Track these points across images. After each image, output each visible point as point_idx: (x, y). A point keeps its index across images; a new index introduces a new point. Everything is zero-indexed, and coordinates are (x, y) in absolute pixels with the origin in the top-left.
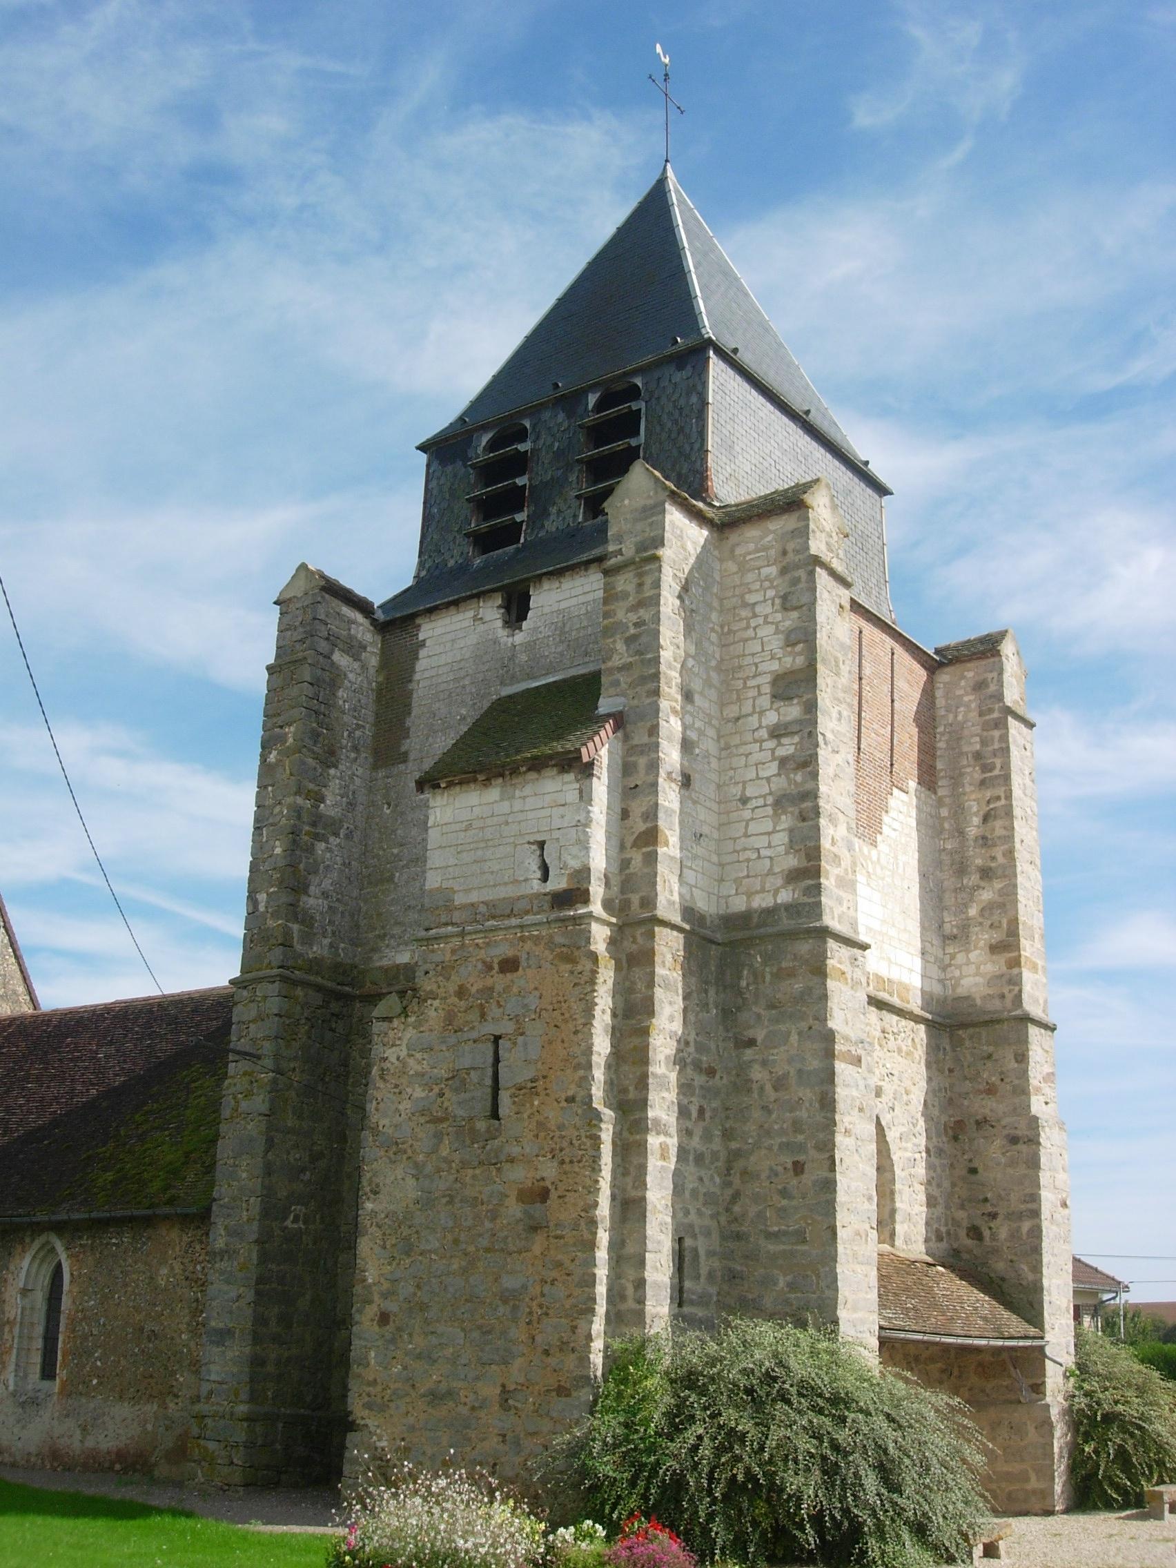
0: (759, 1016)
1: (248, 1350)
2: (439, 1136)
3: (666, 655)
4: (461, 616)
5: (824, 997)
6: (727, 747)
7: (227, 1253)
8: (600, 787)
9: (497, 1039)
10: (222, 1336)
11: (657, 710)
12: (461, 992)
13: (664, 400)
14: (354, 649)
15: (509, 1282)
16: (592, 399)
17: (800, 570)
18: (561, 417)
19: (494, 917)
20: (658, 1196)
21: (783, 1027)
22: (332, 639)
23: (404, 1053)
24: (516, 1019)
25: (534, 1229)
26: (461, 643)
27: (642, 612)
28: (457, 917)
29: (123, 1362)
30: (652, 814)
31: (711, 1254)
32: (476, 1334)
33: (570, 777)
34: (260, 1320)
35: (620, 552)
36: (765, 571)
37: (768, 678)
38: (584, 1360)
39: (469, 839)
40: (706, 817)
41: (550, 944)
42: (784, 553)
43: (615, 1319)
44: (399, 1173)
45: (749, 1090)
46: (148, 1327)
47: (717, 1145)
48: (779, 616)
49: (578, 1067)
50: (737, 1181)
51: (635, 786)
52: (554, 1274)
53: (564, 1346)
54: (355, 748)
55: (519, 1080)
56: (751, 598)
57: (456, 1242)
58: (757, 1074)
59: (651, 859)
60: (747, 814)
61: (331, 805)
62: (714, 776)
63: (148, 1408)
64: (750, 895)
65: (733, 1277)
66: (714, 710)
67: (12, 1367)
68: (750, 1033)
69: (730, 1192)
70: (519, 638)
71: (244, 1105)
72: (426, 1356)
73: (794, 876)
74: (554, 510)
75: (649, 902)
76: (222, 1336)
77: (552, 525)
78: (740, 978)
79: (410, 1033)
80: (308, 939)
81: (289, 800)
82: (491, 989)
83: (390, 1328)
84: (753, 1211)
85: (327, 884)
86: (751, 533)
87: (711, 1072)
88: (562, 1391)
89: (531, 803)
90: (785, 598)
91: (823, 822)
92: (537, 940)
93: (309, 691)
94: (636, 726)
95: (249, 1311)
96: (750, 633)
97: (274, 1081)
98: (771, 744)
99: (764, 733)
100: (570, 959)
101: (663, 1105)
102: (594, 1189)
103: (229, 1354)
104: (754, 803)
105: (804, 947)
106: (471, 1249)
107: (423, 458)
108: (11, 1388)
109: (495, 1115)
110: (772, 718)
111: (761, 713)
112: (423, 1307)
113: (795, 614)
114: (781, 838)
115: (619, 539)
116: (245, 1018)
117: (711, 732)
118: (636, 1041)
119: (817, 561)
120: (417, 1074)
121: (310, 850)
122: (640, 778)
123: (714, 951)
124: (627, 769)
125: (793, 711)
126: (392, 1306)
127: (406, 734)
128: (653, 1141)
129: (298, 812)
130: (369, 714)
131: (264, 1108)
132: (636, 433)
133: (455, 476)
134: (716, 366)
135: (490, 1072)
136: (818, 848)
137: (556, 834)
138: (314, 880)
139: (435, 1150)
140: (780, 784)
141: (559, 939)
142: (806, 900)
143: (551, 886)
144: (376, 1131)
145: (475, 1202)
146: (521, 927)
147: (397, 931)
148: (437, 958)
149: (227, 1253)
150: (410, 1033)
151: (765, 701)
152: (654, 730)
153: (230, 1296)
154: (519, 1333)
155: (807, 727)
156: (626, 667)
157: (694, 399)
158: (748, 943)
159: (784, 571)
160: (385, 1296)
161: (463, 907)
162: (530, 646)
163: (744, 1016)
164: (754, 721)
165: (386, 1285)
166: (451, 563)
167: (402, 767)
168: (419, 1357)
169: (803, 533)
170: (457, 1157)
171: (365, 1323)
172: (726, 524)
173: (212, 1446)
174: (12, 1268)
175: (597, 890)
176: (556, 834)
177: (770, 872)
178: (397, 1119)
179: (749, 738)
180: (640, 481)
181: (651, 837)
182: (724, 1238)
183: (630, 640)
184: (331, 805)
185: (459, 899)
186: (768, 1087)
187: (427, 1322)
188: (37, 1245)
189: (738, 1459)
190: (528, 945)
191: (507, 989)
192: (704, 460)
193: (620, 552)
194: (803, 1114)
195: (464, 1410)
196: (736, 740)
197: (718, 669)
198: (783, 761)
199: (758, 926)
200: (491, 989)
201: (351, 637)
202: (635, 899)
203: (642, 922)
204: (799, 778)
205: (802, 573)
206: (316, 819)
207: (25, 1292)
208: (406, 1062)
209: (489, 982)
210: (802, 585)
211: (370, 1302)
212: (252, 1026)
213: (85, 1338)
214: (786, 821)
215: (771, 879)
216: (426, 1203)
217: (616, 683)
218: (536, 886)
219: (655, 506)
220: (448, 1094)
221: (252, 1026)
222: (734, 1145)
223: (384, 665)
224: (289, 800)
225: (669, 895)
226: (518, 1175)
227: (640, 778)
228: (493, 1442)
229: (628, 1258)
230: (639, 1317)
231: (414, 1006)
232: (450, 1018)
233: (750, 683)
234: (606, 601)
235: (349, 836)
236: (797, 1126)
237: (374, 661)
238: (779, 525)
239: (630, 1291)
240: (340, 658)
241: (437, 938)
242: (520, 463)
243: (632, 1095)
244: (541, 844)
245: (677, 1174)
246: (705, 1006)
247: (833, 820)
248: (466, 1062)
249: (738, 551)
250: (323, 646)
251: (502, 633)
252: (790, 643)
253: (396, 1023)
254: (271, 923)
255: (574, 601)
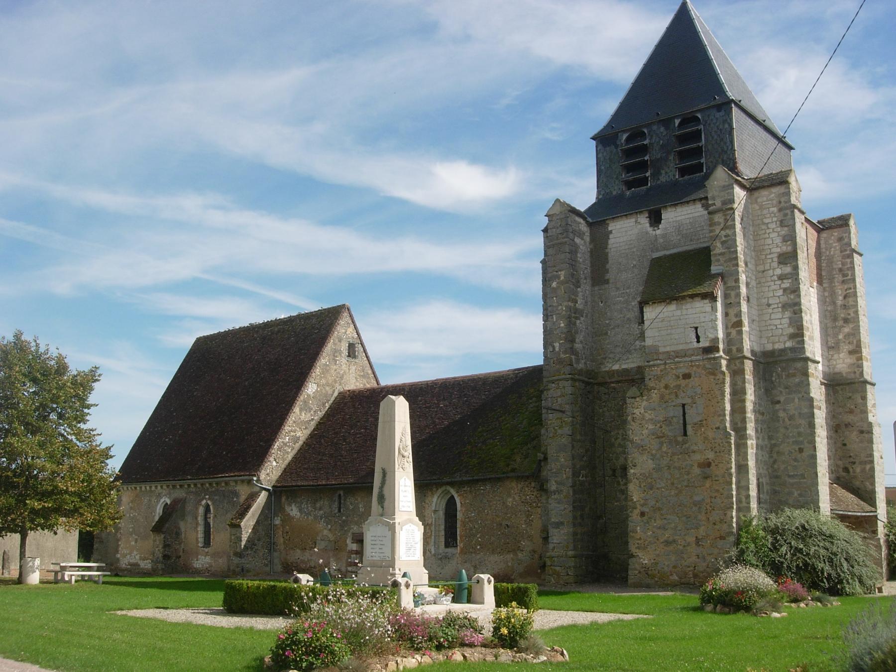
0: (781, 392)
1: (571, 530)
2: (662, 443)
3: (739, 249)
4: (628, 221)
5: (809, 384)
6: (760, 283)
7: (558, 491)
8: (719, 305)
9: (684, 405)
10: (558, 525)
11: (738, 272)
12: (666, 387)
13: (712, 125)
14: (581, 235)
15: (696, 498)
16: (677, 122)
17: (788, 210)
18: (662, 129)
19: (677, 357)
20: (751, 463)
21: (791, 396)
22: (574, 232)
23: (642, 411)
24: (692, 397)
25: (706, 478)
26: (630, 233)
27: (727, 231)
28: (661, 357)
29: (493, 538)
30: (739, 314)
31: (767, 484)
32: (684, 518)
33: (707, 301)
34: (575, 518)
35: (714, 204)
36: (772, 209)
37: (776, 255)
38: (731, 526)
39: (669, 325)
40: (755, 312)
41: (704, 368)
42: (780, 202)
43: (739, 510)
44: (645, 458)
45: (778, 421)
46: (504, 523)
47: (766, 442)
48: (779, 229)
49: (719, 416)
50: (775, 455)
51: (731, 304)
52: (716, 494)
53: (721, 521)
54: (586, 279)
55: (695, 421)
56: (766, 221)
57: (673, 484)
58: (781, 414)
59: (740, 333)
60: (770, 311)
61: (580, 305)
62: (755, 295)
63: (508, 556)
64: (773, 343)
65: (775, 492)
66: (754, 268)
67: (432, 543)
68: (778, 398)
69: (772, 460)
70: (658, 232)
71: (559, 431)
72: (663, 528)
73: (792, 336)
74: (663, 172)
75: (740, 350)
76: (558, 525)
77: (663, 178)
78: (772, 376)
79: (644, 403)
80: (578, 361)
81: (566, 303)
82: (680, 386)
83: (646, 517)
84: (782, 467)
85: (581, 338)
86: (764, 192)
87: (763, 414)
88: (722, 538)
89: (690, 311)
90: (781, 221)
91: (803, 314)
92: (698, 366)
93: (568, 256)
94: (729, 277)
95: (571, 514)
96: (767, 235)
97: (573, 422)
98: (779, 282)
99: (775, 278)
100: (714, 374)
101: (751, 430)
102: (730, 462)
103: (562, 532)
104: (773, 306)
105: (799, 365)
106: (679, 486)
107: (594, 143)
108: (433, 552)
109: (685, 434)
110: (778, 272)
111: (774, 269)
112: (659, 509)
113: (786, 229)
114: (786, 321)
115: (714, 198)
116: (555, 395)
117: (754, 278)
118: (740, 404)
119: (794, 207)
120: (649, 419)
121: (575, 324)
122: (732, 300)
123: (761, 366)
124: (726, 296)
125: (788, 269)
126: (646, 509)
127: (607, 271)
128: (749, 442)
129: (569, 308)
130: (588, 262)
131: (570, 433)
132: (700, 139)
133: (611, 152)
134: (735, 111)
135: (682, 418)
136: (802, 325)
137: (703, 324)
138: (577, 336)
139: (660, 448)
140: (784, 299)
141: (708, 366)
142: (797, 346)
143: (701, 345)
144: (632, 442)
145: (679, 468)
146: (691, 361)
147: (611, 356)
148: (654, 373)
149: (558, 491)
150: (644, 403)
151: (775, 264)
152: (737, 280)
153: (559, 507)
154: (702, 517)
155: (794, 275)
156: (722, 254)
157: (727, 126)
158: (776, 362)
159: (780, 210)
160: (642, 506)
161: (664, 353)
162: (664, 236)
163: (774, 392)
164: (771, 272)
165: (642, 502)
166: (614, 193)
167: (607, 286)
168: (659, 528)
169: (788, 194)
170: (670, 451)
171: (635, 516)
172: (753, 187)
173: (558, 568)
174: (427, 501)
175: (721, 346)
176: (703, 324)
177: (782, 335)
178: (642, 437)
179: (769, 279)
180: (720, 174)
181: (739, 324)
182: (771, 478)
183: (723, 243)
184: (580, 305)
185: (661, 350)
186: (786, 419)
187: (662, 515)
188: (440, 491)
189: (799, 558)
190: (695, 368)
191: (686, 385)
192: (734, 154)
193: (714, 204)
194: (802, 430)
195: (681, 547)
196: (763, 280)
197: (754, 251)
198: (785, 290)
199: (778, 356)
200: (680, 386)
201: (580, 230)
202: (734, 349)
203: (739, 358)
204: (792, 297)
205: (788, 211)
206: (576, 311)
207: (435, 511)
208: (644, 416)
209: (678, 383)
210: (789, 217)
211: (636, 508)
212: (559, 399)
213: (471, 529)
214: (787, 314)
215: (782, 337)
216: (658, 469)
217: (718, 260)
218: (695, 345)
219: (729, 185)
220: (664, 427)
221: (559, 399)
222: (773, 442)
223: (593, 240)
224: (566, 303)
225: (747, 345)
226: (698, 457)
227: (732, 300)
228: (694, 558)
229: (743, 488)
230: (748, 509)
231: (646, 392)
232: (662, 397)
233: (768, 257)
234: (711, 225)
235: (587, 316)
236: (799, 434)
237: (588, 239)
238: (776, 190)
239: (744, 500)
240: (577, 240)
241: (654, 366)
242: (644, 149)
243: (739, 425)
244: (696, 328)
245: (756, 454)
246: (760, 388)
247: (806, 314)
248: (671, 414)
249: (759, 200)
250: (571, 235)
251: (650, 229)
252: (785, 240)
253: (638, 399)
254: (562, 356)
255: (683, 217)
